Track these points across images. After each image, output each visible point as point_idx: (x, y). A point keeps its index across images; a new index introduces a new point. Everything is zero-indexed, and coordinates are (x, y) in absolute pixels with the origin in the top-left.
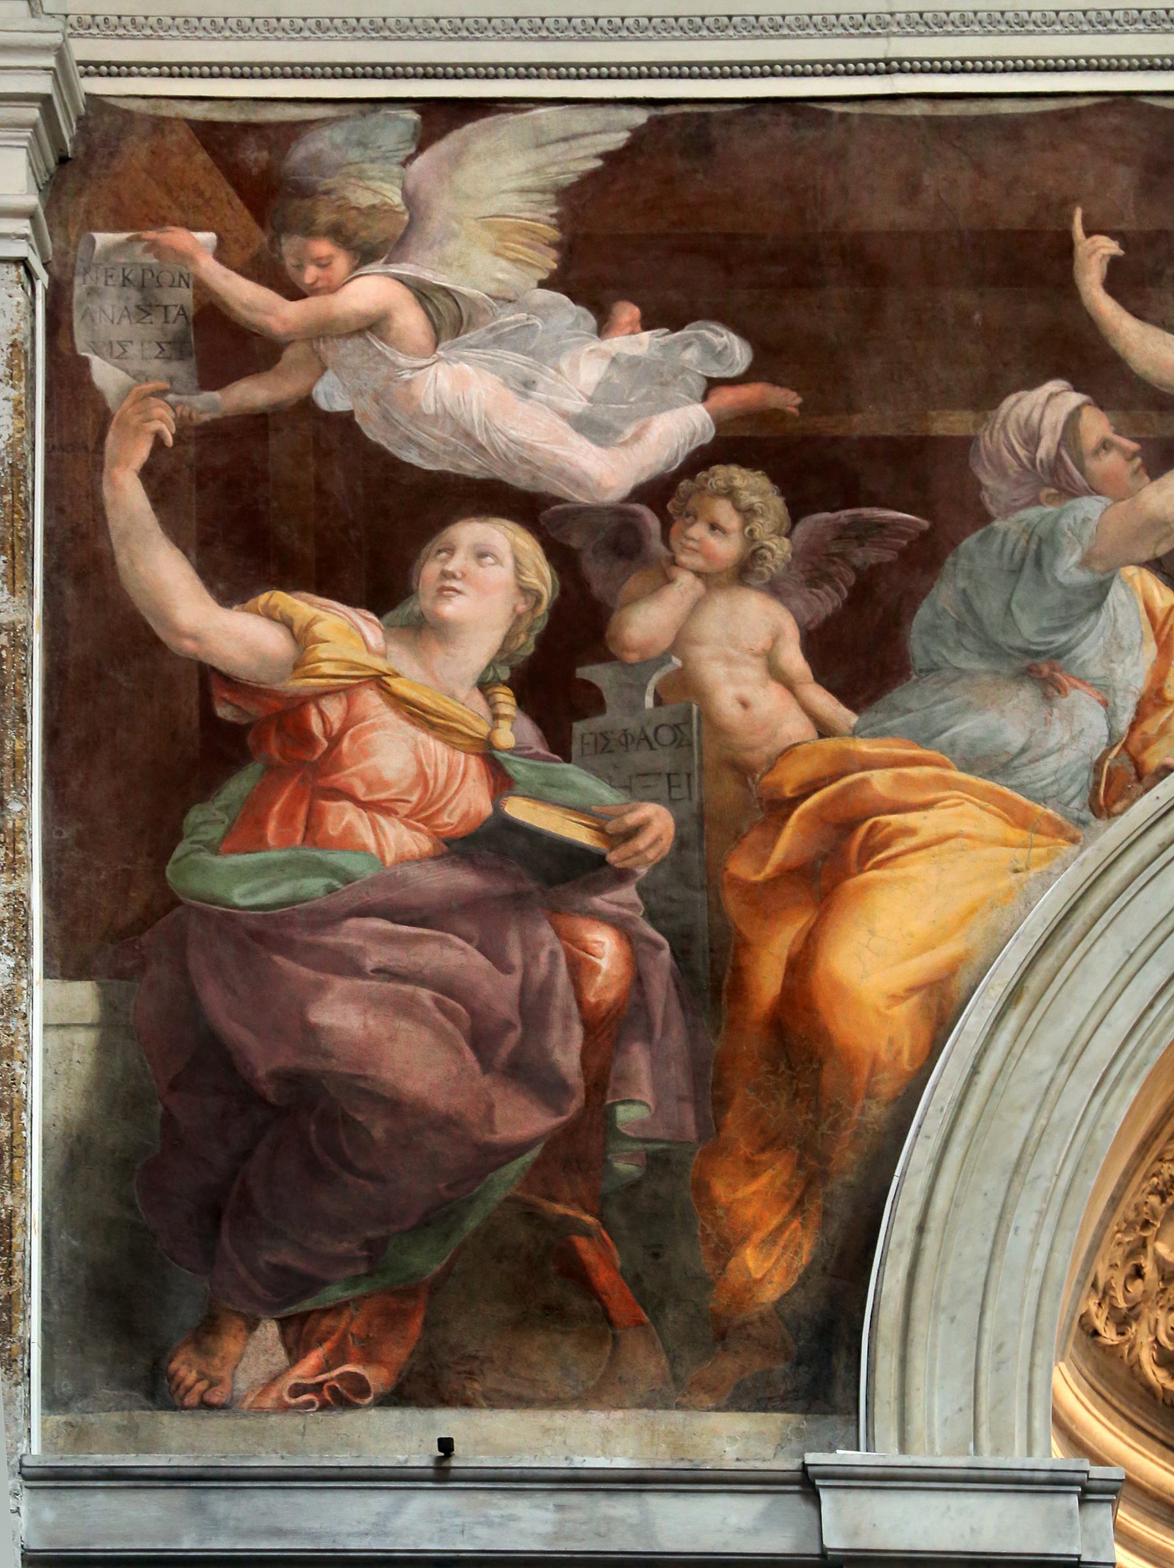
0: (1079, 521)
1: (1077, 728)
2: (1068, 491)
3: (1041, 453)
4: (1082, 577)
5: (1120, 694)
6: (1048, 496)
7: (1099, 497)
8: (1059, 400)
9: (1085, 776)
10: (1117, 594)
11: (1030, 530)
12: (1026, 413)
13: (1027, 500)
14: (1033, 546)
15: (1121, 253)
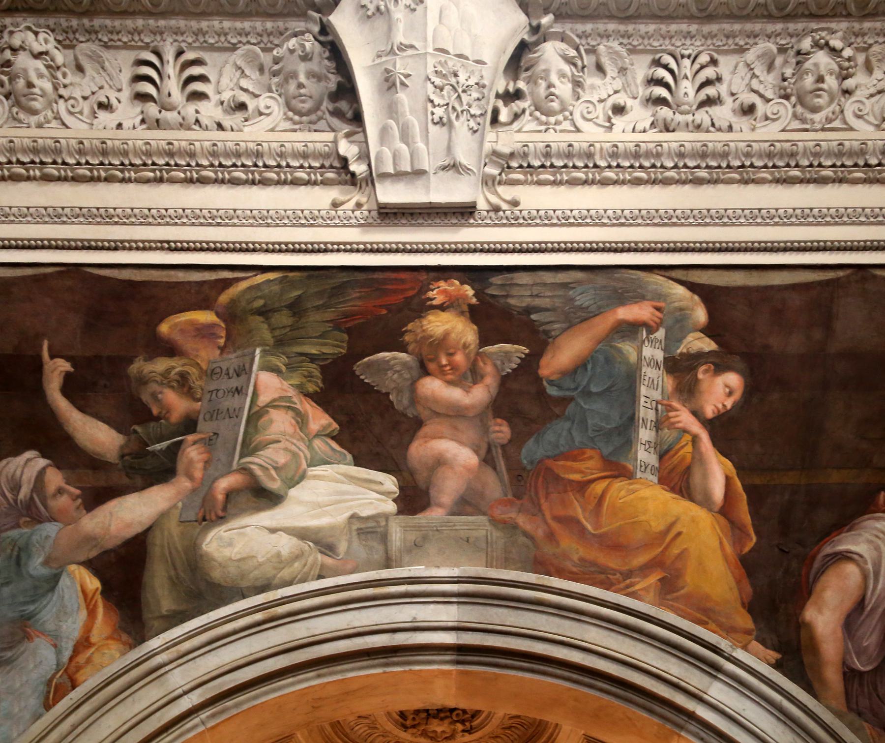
0: (43, 537)
1: (38, 660)
2: (37, 519)
3: (21, 496)
4: (45, 571)
5: (64, 640)
6: (25, 522)
7: (56, 523)
8: (33, 463)
9: (42, 688)
10: (64, 581)
11: (14, 542)
12: (12, 471)
13: (12, 524)
14: (15, 553)
15: (72, 370)
